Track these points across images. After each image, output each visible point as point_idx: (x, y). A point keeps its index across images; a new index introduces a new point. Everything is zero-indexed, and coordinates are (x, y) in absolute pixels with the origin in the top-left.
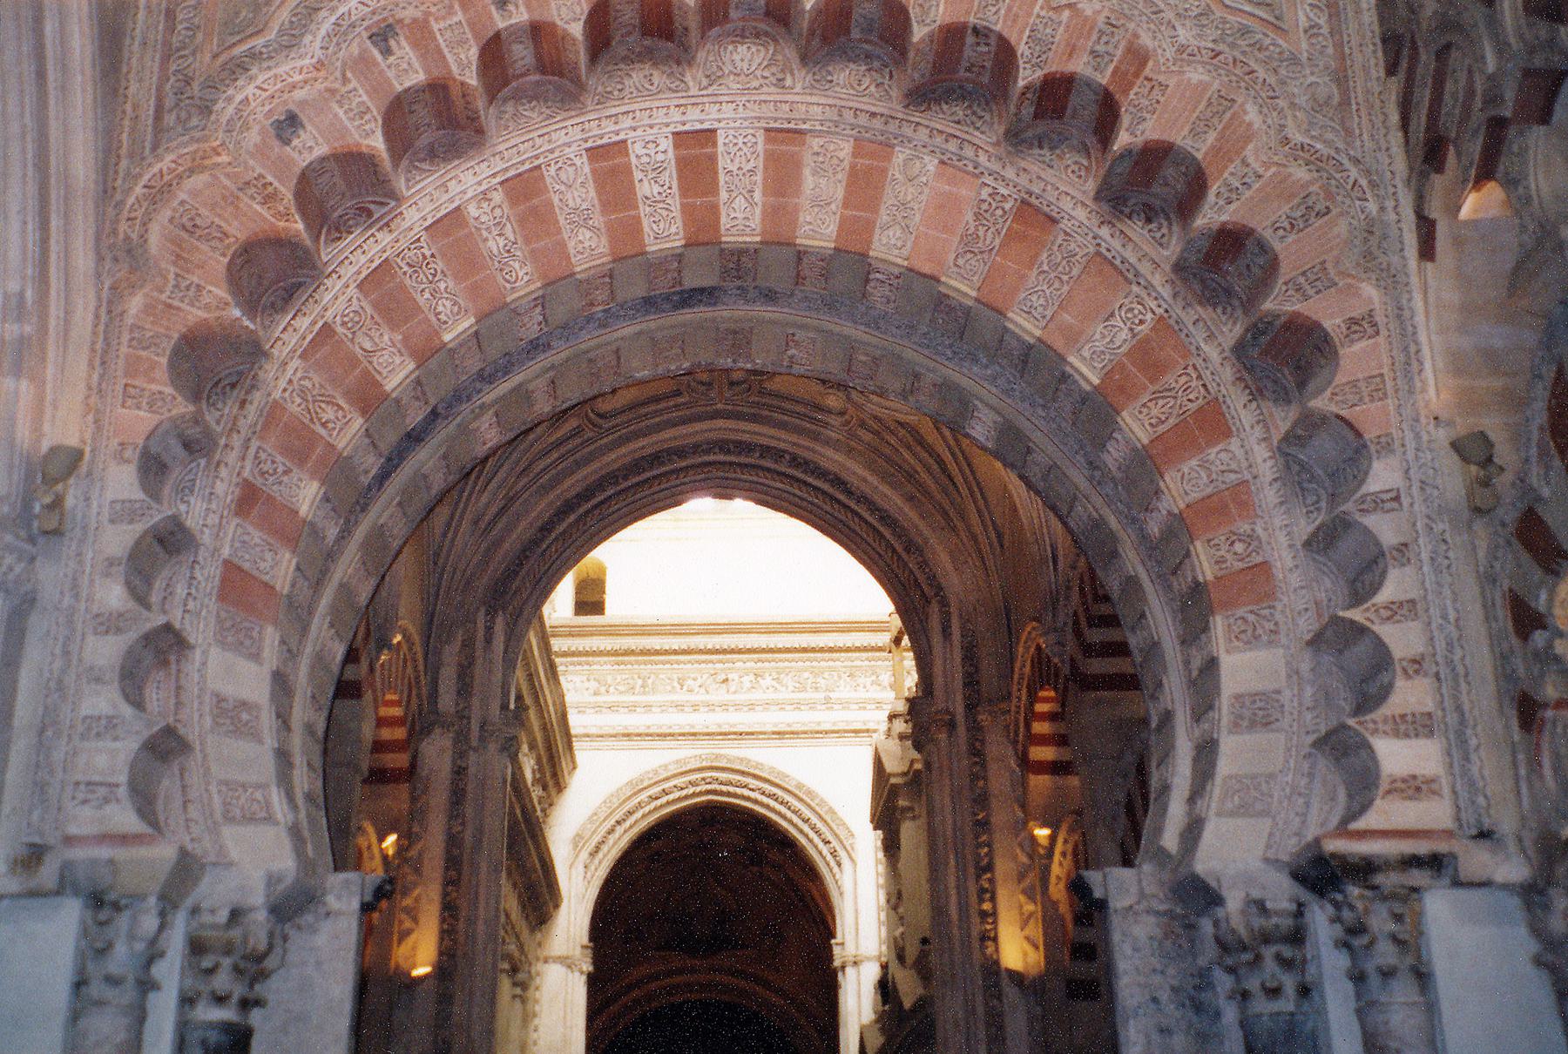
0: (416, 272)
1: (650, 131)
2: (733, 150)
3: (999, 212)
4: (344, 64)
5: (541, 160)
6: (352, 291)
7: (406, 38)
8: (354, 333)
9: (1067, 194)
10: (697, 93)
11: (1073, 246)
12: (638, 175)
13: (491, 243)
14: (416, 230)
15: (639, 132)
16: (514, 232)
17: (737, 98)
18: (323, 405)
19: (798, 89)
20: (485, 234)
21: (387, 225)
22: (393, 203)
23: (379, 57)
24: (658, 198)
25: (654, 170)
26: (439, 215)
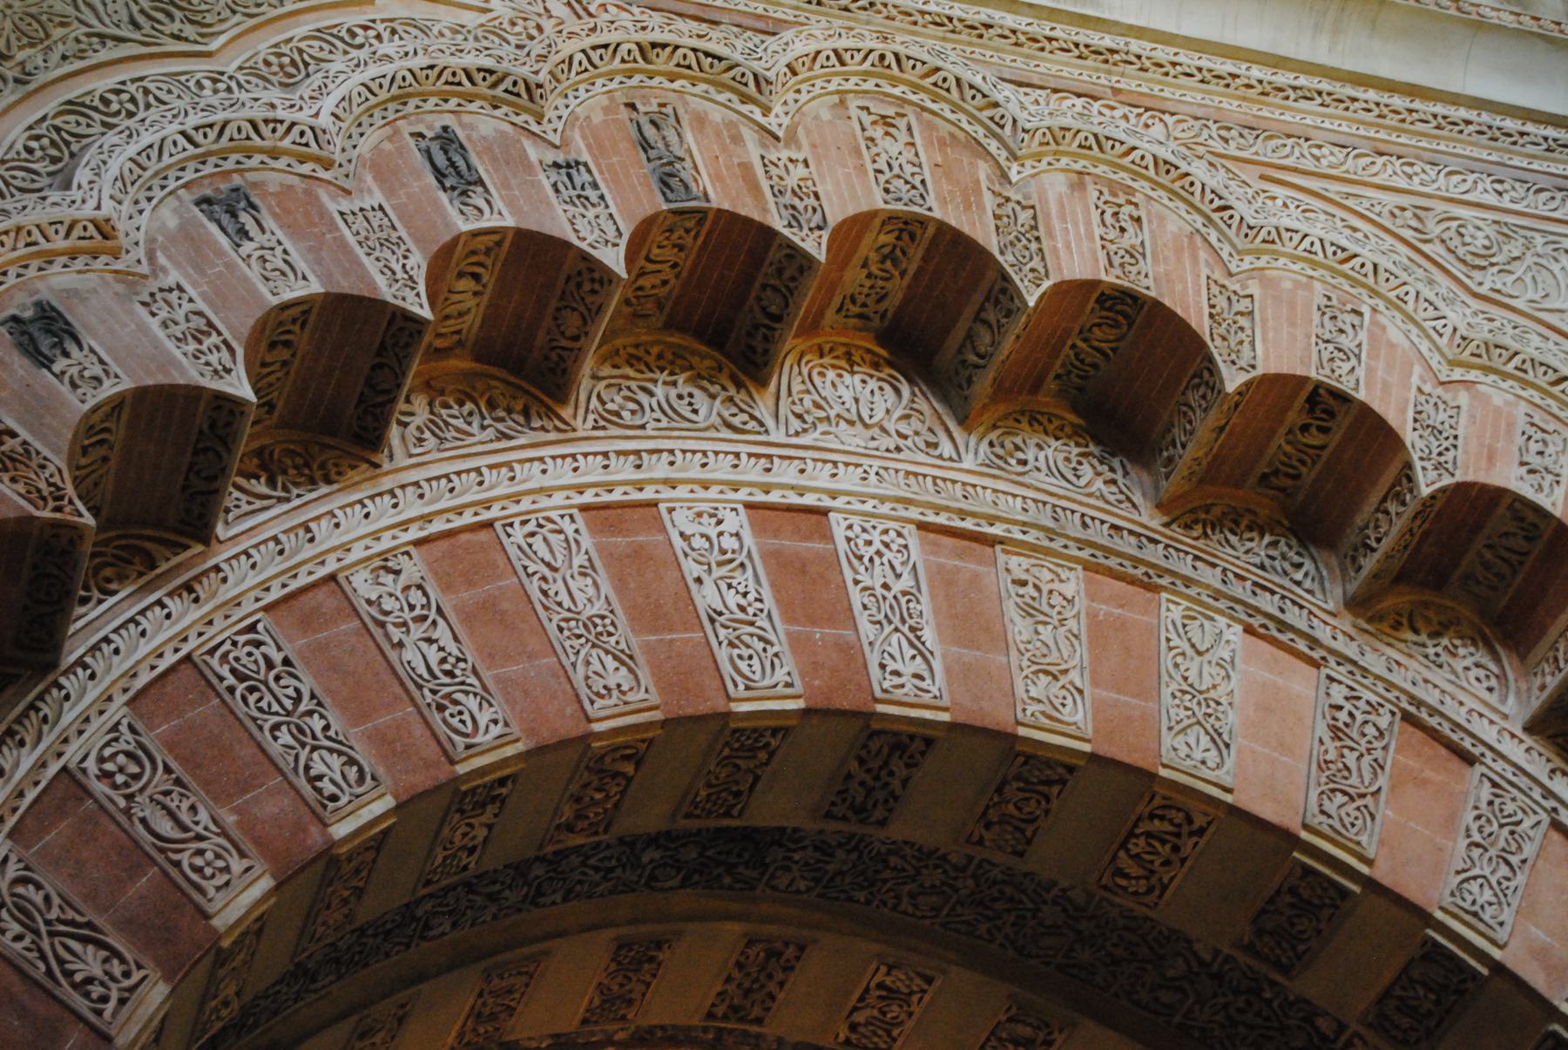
0: (252, 690)
1: (701, 494)
2: (867, 552)
3: (1370, 730)
4: (151, 241)
5: (495, 512)
6: (117, 710)
7: (275, 216)
8: (130, 798)
9: (1481, 715)
10: (784, 440)
11: (1510, 808)
12: (692, 569)
13: (410, 654)
14: (248, 606)
15: (682, 492)
16: (456, 639)
17: (865, 461)
18: (75, 945)
19: (969, 463)
20: (397, 635)
21: (188, 587)
22: (199, 548)
23: (224, 241)
24: (741, 616)
25: (720, 564)
26: (294, 585)
